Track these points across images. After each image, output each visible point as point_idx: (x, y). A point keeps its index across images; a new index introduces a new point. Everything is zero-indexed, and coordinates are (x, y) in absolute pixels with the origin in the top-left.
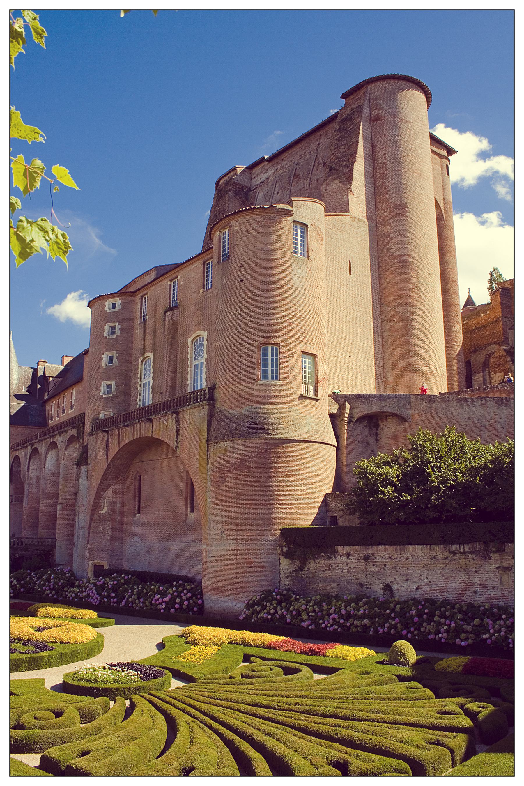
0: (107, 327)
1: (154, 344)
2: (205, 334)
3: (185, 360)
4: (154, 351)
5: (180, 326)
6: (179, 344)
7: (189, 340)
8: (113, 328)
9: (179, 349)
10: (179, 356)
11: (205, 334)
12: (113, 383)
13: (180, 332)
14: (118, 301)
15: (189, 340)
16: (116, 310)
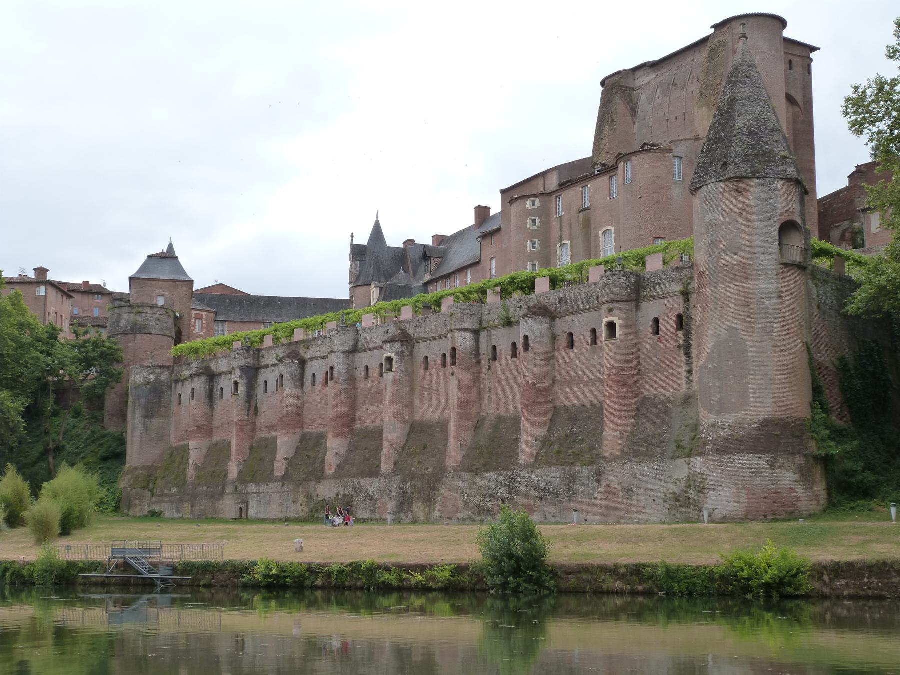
0: (529, 221)
1: (571, 235)
2: (613, 229)
3: (597, 247)
4: (571, 239)
5: (592, 222)
6: (593, 235)
7: (601, 233)
8: (534, 221)
9: (593, 239)
10: (593, 244)
11: (613, 229)
12: (537, 264)
13: (593, 226)
14: (537, 201)
15: (601, 233)
16: (536, 207)
